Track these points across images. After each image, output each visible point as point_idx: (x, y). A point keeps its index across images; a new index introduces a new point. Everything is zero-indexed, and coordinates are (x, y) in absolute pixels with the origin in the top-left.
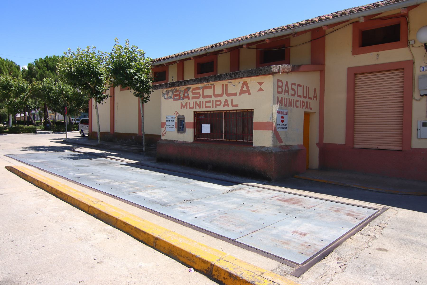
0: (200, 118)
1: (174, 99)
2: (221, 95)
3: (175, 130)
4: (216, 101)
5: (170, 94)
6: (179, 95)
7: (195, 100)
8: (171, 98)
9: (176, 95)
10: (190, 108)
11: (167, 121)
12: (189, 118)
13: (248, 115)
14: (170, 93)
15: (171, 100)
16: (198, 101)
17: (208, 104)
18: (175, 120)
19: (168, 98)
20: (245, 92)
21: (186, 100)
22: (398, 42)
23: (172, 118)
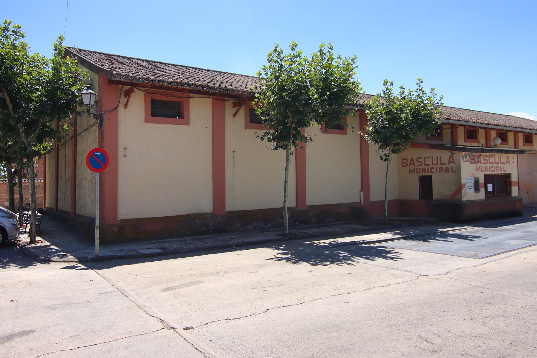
0: (489, 178)
1: (471, 163)
2: (437, 164)
3: (473, 190)
4: (440, 168)
5: (468, 158)
6: (474, 159)
7: (485, 165)
8: (468, 161)
9: (472, 159)
10: (417, 173)
11: (467, 183)
12: (482, 180)
13: (508, 176)
14: (468, 157)
15: (469, 163)
16: (487, 165)
17: (493, 169)
18: (473, 182)
19: (466, 161)
20: (452, 162)
21: (479, 164)
22: (344, 136)
23: (471, 179)
